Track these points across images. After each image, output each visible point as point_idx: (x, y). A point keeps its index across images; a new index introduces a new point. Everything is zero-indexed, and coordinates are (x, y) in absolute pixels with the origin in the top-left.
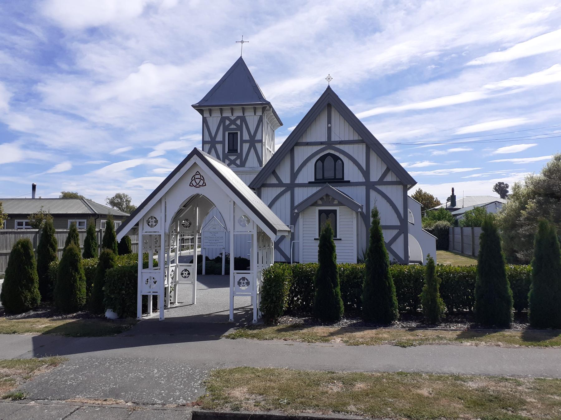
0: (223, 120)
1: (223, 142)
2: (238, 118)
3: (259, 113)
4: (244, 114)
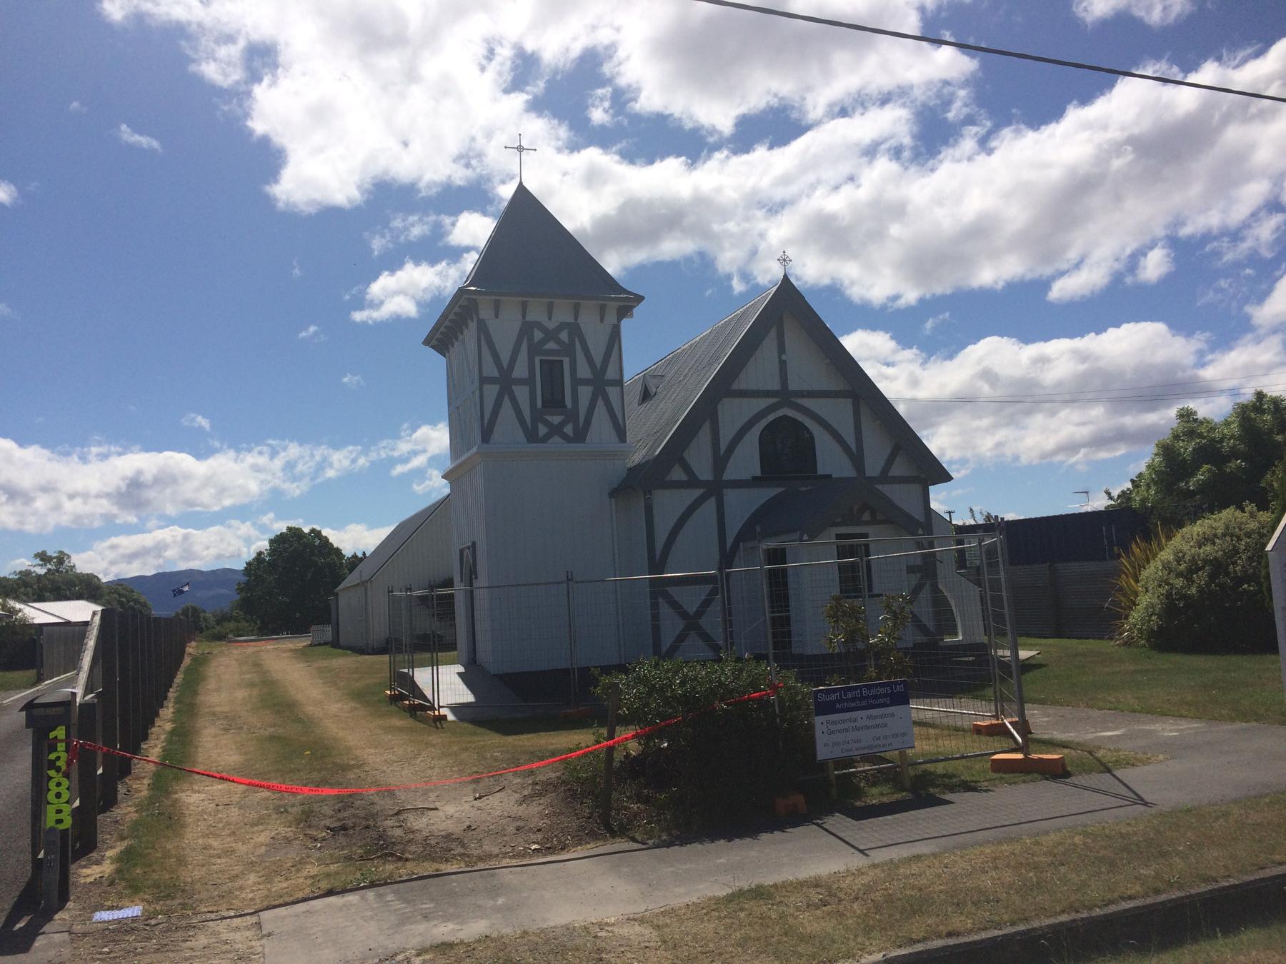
0: (527, 328)
2: (562, 326)
3: (611, 318)
4: (576, 318)
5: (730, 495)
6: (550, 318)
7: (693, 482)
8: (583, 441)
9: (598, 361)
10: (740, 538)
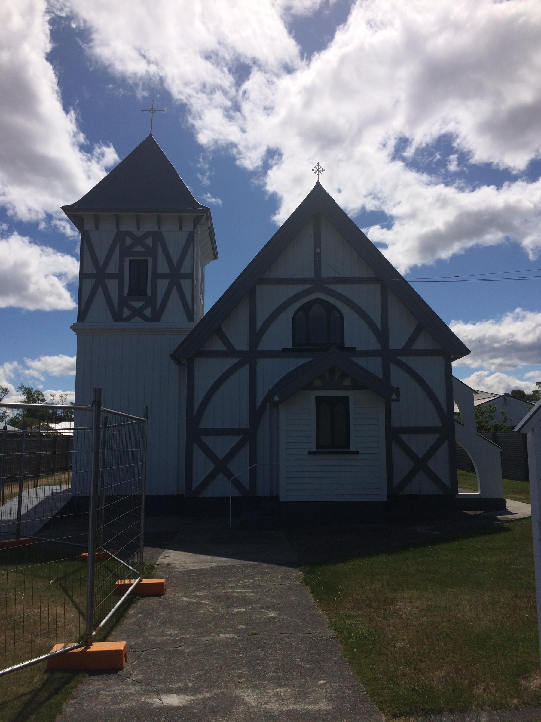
0: (120, 236)
1: (119, 276)
2: (148, 234)
3: (188, 227)
4: (159, 228)
5: (263, 364)
6: (138, 229)
7: (231, 352)
8: (159, 321)
9: (175, 259)
10: (268, 399)
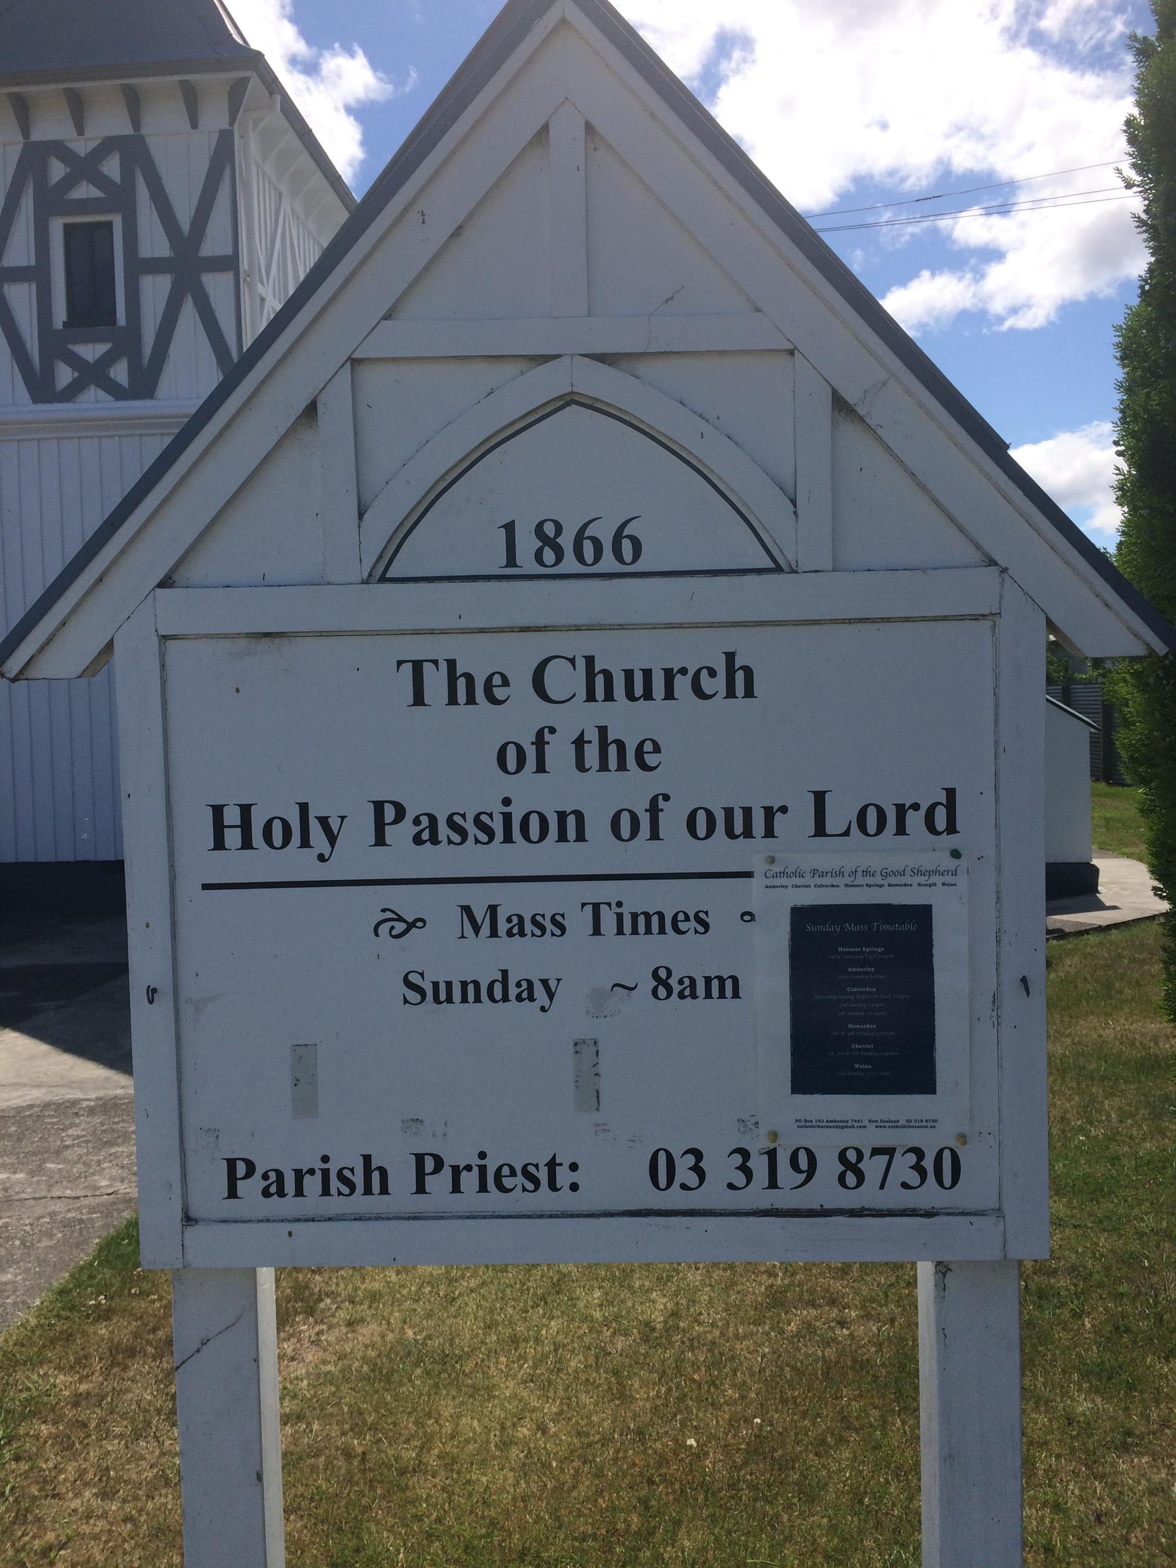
1: (38, 274)
2: (109, 145)
3: (214, 117)
4: (136, 124)
6: (80, 131)
